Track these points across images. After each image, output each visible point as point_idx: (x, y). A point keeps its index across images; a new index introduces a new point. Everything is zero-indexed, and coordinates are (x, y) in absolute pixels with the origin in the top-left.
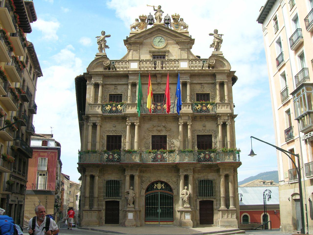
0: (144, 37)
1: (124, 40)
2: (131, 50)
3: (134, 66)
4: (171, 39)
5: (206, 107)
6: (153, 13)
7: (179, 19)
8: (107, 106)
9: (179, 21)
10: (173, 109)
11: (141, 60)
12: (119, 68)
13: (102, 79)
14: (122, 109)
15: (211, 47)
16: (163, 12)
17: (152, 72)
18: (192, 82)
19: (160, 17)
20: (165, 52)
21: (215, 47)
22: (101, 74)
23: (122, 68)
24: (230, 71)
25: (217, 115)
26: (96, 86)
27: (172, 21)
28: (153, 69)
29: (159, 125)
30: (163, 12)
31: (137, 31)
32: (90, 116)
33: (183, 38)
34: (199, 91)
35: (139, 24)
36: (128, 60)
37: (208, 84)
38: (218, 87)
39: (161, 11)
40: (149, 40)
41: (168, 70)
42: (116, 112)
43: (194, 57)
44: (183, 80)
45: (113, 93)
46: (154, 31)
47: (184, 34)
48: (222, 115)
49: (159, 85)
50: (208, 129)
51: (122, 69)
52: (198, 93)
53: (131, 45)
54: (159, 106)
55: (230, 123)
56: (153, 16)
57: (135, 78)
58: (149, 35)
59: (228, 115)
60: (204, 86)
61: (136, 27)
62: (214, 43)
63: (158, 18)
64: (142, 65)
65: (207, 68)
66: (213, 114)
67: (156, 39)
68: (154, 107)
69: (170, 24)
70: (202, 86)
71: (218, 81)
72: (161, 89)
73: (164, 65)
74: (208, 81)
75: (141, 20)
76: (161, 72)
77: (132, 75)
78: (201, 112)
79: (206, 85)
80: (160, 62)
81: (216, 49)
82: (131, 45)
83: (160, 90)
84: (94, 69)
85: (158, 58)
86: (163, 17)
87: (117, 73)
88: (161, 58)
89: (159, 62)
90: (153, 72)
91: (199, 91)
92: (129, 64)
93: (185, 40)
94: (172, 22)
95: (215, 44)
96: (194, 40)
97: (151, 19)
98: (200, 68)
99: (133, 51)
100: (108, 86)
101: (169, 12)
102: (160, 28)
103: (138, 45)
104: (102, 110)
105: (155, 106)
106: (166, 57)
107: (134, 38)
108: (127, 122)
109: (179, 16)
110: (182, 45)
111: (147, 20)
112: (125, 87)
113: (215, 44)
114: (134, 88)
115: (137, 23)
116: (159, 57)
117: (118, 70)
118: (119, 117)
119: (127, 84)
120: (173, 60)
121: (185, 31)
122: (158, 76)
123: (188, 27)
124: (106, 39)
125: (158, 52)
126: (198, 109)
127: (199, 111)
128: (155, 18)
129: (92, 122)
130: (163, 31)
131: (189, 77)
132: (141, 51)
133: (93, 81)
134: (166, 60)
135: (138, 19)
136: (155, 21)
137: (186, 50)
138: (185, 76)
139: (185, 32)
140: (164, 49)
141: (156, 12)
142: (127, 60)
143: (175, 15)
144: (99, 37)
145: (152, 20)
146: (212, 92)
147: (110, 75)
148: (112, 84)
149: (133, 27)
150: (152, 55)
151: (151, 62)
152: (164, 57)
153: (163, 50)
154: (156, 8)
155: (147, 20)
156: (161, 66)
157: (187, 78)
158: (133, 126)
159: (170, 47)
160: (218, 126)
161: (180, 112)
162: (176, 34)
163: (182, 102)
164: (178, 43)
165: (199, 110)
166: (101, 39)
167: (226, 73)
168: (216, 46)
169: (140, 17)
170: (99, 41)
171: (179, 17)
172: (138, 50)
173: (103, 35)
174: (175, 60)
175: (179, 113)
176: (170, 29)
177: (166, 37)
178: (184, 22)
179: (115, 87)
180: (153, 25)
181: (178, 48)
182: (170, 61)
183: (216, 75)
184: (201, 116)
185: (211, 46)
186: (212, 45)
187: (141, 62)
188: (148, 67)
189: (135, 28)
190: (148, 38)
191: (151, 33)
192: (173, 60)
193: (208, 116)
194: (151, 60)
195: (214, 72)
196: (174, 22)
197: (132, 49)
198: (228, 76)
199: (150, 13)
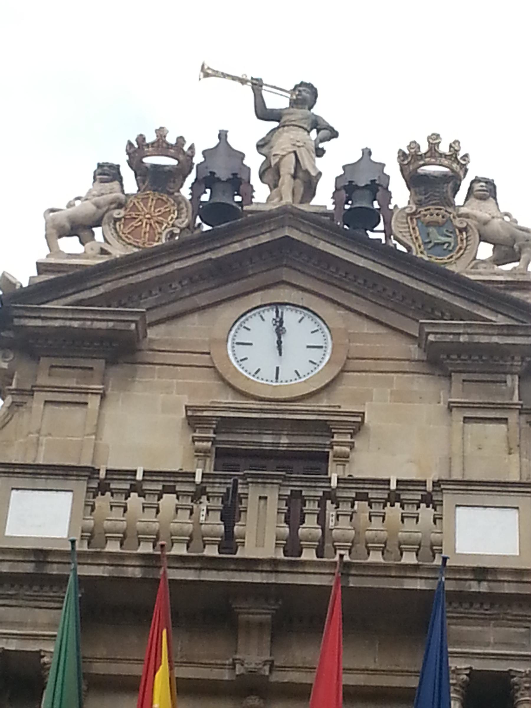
2: (31, 393)
4: (382, 330)
6: (248, 135)
7: (456, 189)
9: (460, 198)
11: (102, 474)
16: (334, 134)
19: (306, 164)
20: (324, 428)
27: (400, 195)
30: (334, 134)
33: (494, 319)
35: (120, 205)
39: (317, 124)
40: (192, 330)
44: (478, 665)
56: (242, 156)
57: (35, 625)
61: (98, 231)
63: (283, 171)
64: (115, 520)
67: (253, 321)
69: (381, 226)
73: (310, 527)
75: (142, 173)
76: (272, 579)
77: (10, 597)
86: (329, 168)
93: (510, 340)
94: (400, 206)
97: (223, 174)
99: (46, 402)
101: (370, 129)
102: (296, 235)
103: (99, 364)
107: (69, 299)
109: (456, 159)
110: (475, 377)
111: (191, 178)
121: (509, 273)
122: (243, 617)
125: (262, 425)
128: (262, 176)
132: (110, 412)
134: (334, 483)
135: (117, 168)
136: (261, 193)
138: (492, 633)
139: (510, 279)
140: (323, 404)
141: (274, 130)
143: (424, 148)
145: (239, 182)
149: (68, 226)
150: (208, 445)
151: (196, 497)
152: (316, 462)
153: (308, 412)
154: (276, 101)
155: (191, 178)
157: (508, 644)
159: (375, 390)
162: (431, 291)
164: (439, 361)
169: (136, 151)
172: (94, 402)
177: (342, 312)
178: (503, 209)
181: (443, 405)
182: (362, 497)
187: (103, 488)
194: (198, 479)
196: (419, 204)
197: (42, 389)
199: (223, 135)
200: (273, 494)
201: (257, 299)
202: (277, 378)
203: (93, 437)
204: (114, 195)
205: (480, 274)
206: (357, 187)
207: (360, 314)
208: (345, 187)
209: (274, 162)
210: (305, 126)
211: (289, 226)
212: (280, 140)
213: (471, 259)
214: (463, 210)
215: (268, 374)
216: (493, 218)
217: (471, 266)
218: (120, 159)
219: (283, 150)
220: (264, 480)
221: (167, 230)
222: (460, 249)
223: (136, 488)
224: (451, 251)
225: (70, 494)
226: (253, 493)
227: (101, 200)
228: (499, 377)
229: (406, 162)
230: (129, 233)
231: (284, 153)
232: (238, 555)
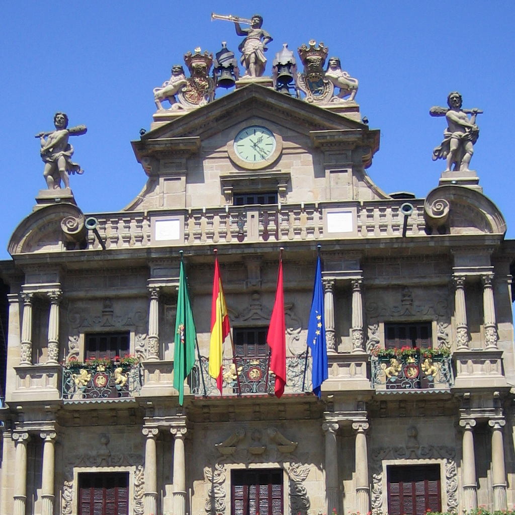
0: (201, 131)
1: (134, 144)
3: (167, 233)
4: (295, 134)
5: (419, 368)
7: (323, 64)
8: (78, 373)
9: (325, 68)
10: (302, 376)
12: (116, 240)
13: (58, 280)
14: (128, 381)
15: (438, 157)
16: (271, 39)
17: (230, 253)
18: (372, 282)
21: (452, 158)
22: (57, 264)
23: (127, 239)
24: (505, 239)
25: (457, 395)
26: (40, 305)
28: (235, 241)
29: (257, 435)
30: (271, 39)
31: (180, 108)
32: (18, 407)
34: (395, 314)
36: (148, 212)
37: (427, 287)
38: (460, 296)
41: (285, 244)
42: (106, 392)
43: (376, 196)
45: (98, 329)
46: (237, 109)
47: (342, 114)
48: (472, 394)
49: (256, 296)
50: (426, 446)
51: (126, 246)
52: (392, 319)
53: (158, 160)
54: (255, 370)
55: (503, 423)
58: (221, 121)
59: (496, 393)
60: (413, 295)
62: (448, 143)
65: (423, 233)
66: (443, 392)
68: (237, 371)
70: (404, 296)
71: (460, 277)
72: (261, 309)
74: (424, 277)
75: (191, 69)
76: (259, 251)
78: (399, 387)
79: (420, 292)
80: (256, 213)
81: (454, 165)
82: (158, 160)
83: (259, 311)
84: (31, 247)
85: (250, 201)
87: (110, 257)
88: (261, 201)
89: (253, 216)
90: (234, 251)
91: (395, 314)
92: (149, 226)
95: (453, 147)
96: (377, 132)
98: (398, 234)
100: (80, 305)
104: (59, 387)
105: (240, 368)
106: (281, 201)
107: (168, 135)
108: (148, 424)
112: (138, 305)
113: (454, 146)
114: (171, 309)
115: (180, 79)
116: (256, 197)
117: (113, 246)
118: (121, 410)
119: (147, 298)
120: (303, 207)
121: (346, 103)
123: (357, 89)
124: (72, 140)
125: (253, 181)
126: (390, 376)
127: (395, 382)
129: (26, 429)
130: (270, 106)
131: (359, 267)
133: (30, 289)
134: (280, 208)
135: (181, 68)
137: (350, 170)
142: (144, 213)
144: (47, 135)
146: (443, 315)
147: (85, 266)
148: (95, 299)
149: (164, 98)
156: (262, 228)
158: (165, 440)
159: (294, 161)
160: (461, 431)
161: (325, 387)
163: (328, 354)
165: (393, 380)
166: (54, 141)
167: (491, 246)
168: (455, 152)
170: (47, 150)
171: (326, 54)
173: (59, 128)
174: (310, 208)
175: (317, 390)
176: (294, 100)
179: (105, 307)
180: (234, 89)
183: (453, 257)
184: (401, 401)
185: (439, 154)
186: (439, 151)
188: (218, 233)
189: (171, 99)
190: (215, 134)
191: (227, 115)
192: (303, 207)
193: (424, 401)
194: (227, 210)
195: (447, 244)
197: (163, 175)
198: (496, 260)
200: (256, 213)
201: (244, 125)
202: (255, 160)
203: (185, 193)
204: (181, 81)
205: (334, 104)
206: (282, 65)
207: (287, 128)
208: (277, 65)
209: (247, 57)
210: (258, 38)
211: (255, 91)
212: (248, 47)
213: (331, 97)
214: (327, 74)
215: (251, 158)
216: (339, 77)
217: (331, 100)
218: (182, 63)
219: (249, 51)
220: (252, 209)
221: (205, 94)
222: (326, 92)
223: (203, 214)
224: (322, 94)
225: (178, 222)
226: (249, 214)
227: (176, 84)
228: (343, 152)
229: (301, 54)
230: (190, 98)
231: (250, 53)
232: (243, 242)
